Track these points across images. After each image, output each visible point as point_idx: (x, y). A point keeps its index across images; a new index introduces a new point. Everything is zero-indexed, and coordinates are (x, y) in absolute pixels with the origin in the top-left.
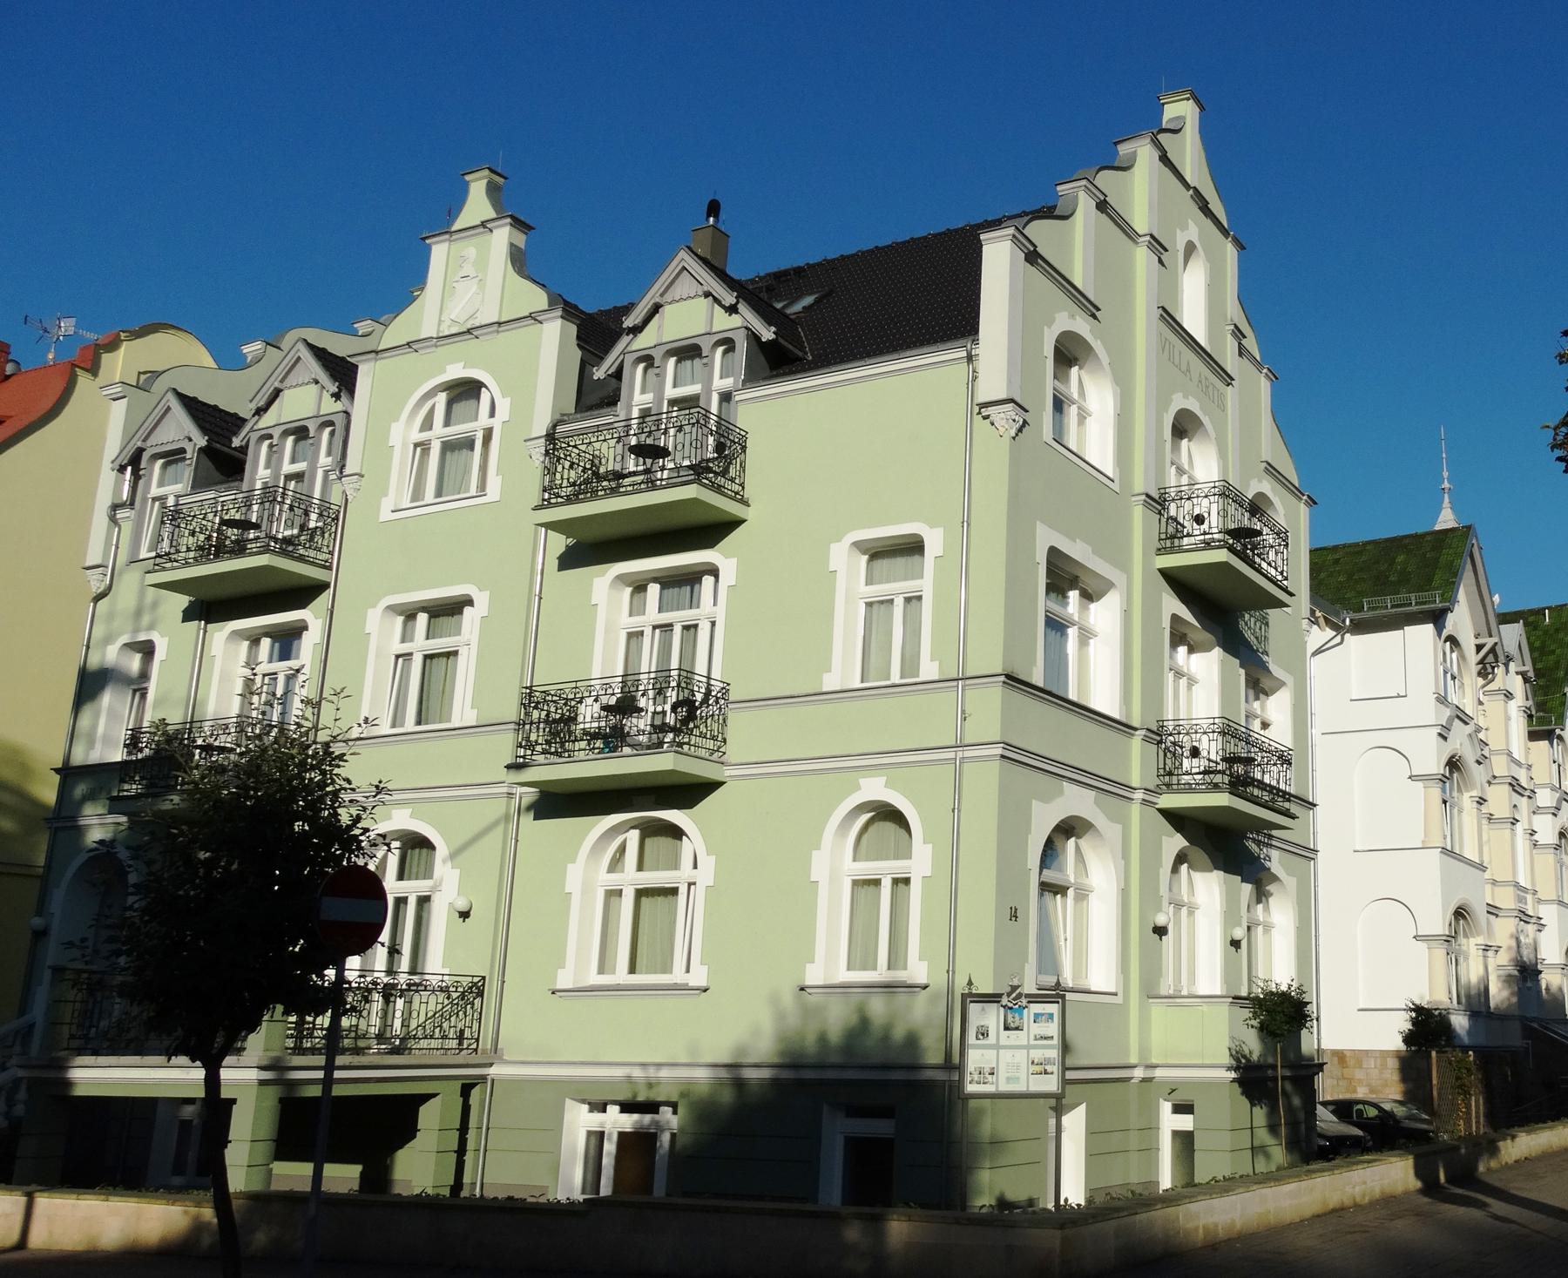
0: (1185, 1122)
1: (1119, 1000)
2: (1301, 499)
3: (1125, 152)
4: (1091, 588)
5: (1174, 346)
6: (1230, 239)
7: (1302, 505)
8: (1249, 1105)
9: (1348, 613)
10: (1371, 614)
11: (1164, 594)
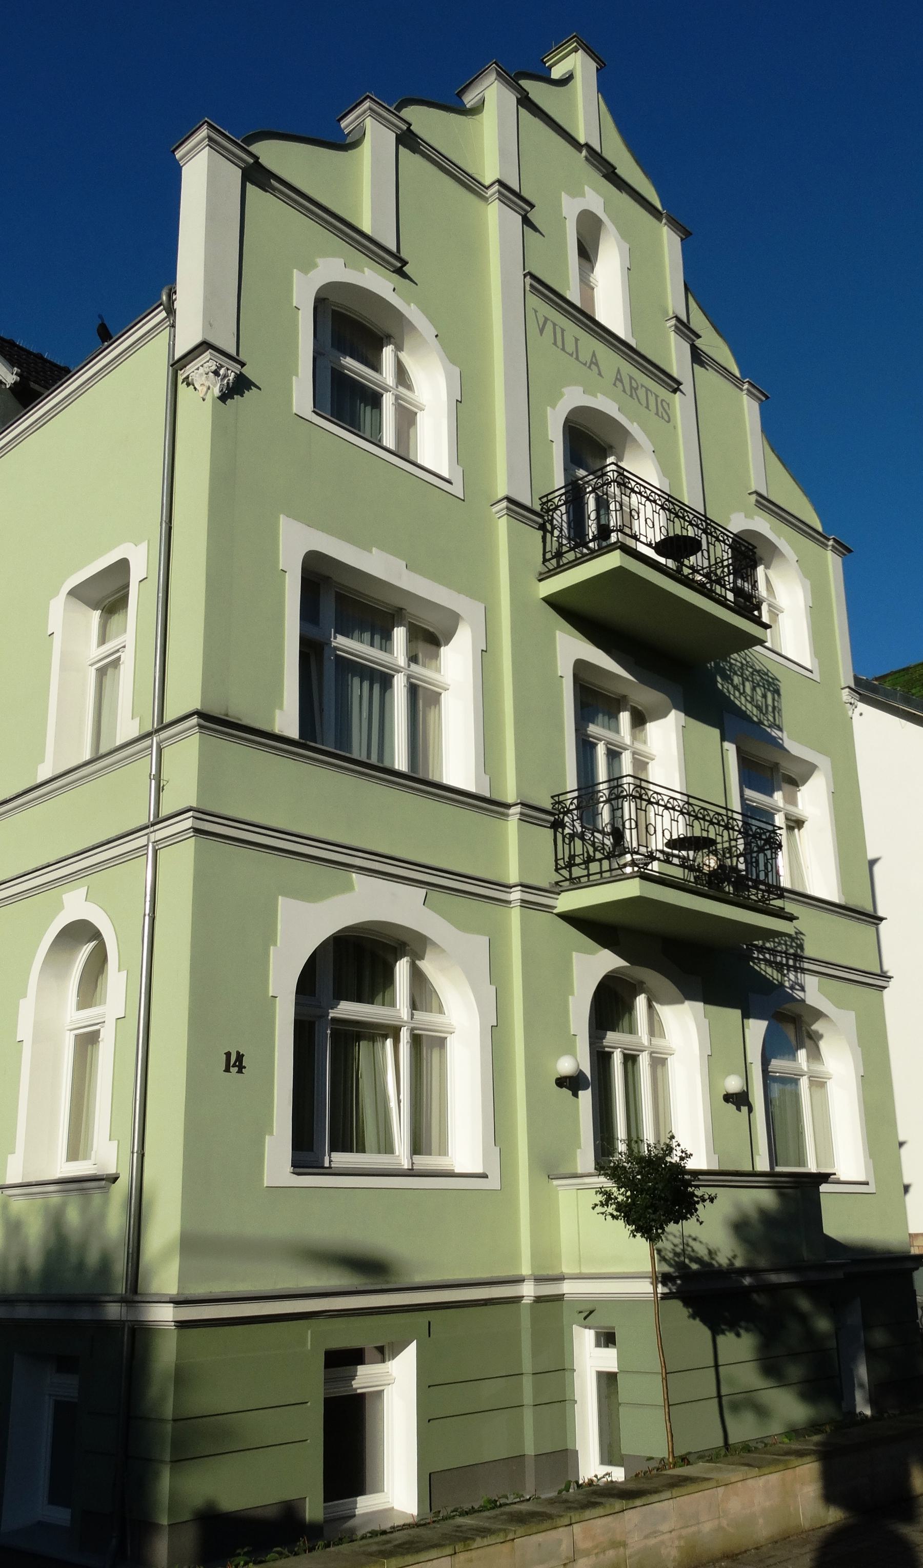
2: (827, 546)
3: (472, 103)
4: (430, 622)
5: (563, 331)
6: (664, 221)
11: (558, 634)
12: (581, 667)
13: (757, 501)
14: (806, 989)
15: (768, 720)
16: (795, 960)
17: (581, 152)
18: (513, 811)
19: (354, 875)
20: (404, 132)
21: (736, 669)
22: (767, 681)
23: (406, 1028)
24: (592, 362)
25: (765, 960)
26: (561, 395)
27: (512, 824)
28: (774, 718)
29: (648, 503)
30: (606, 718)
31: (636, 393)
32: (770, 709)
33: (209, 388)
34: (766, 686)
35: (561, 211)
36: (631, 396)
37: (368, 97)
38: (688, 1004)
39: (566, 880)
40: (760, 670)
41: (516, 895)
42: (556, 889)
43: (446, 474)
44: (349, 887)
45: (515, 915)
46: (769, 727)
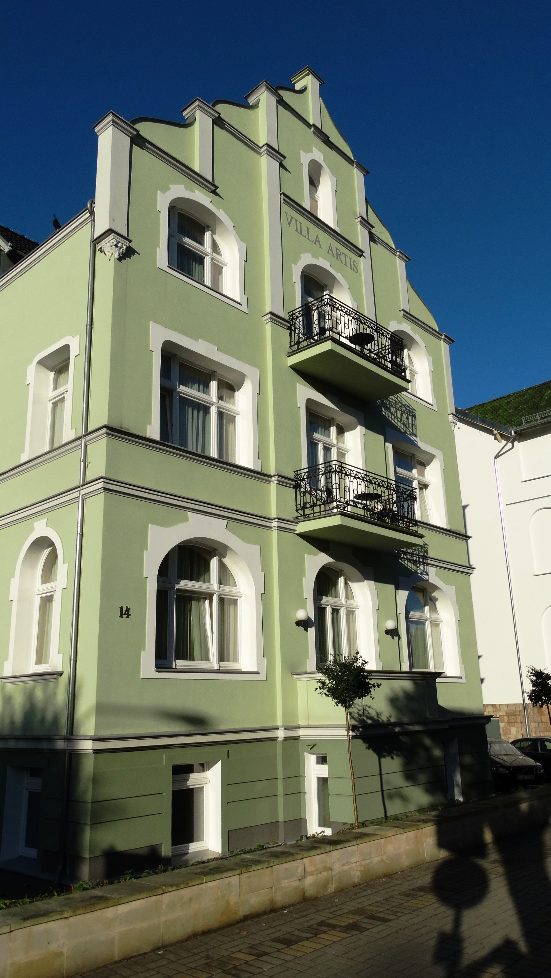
0: (323, 771)
1: (262, 677)
2: (441, 339)
3: (253, 102)
4: (230, 379)
5: (301, 224)
6: (355, 165)
7: (442, 343)
8: (376, 757)
9: (513, 428)
10: (527, 426)
11: (298, 384)
12: (310, 403)
13: (404, 315)
14: (429, 574)
15: (409, 431)
16: (423, 559)
17: (311, 129)
18: (273, 479)
19: (189, 513)
20: (216, 118)
21: (392, 404)
22: (409, 410)
23: (216, 594)
24: (316, 240)
25: (407, 559)
26: (300, 258)
27: (273, 486)
28: (413, 430)
29: (346, 315)
30: (323, 430)
31: (340, 257)
32: (410, 425)
33: (112, 254)
34: (408, 413)
35: (299, 159)
36: (337, 259)
37: (197, 99)
38: (366, 582)
39: (302, 516)
40: (405, 405)
41: (275, 524)
42: (296, 521)
43: (238, 300)
44: (186, 519)
45: (274, 534)
46: (410, 435)
